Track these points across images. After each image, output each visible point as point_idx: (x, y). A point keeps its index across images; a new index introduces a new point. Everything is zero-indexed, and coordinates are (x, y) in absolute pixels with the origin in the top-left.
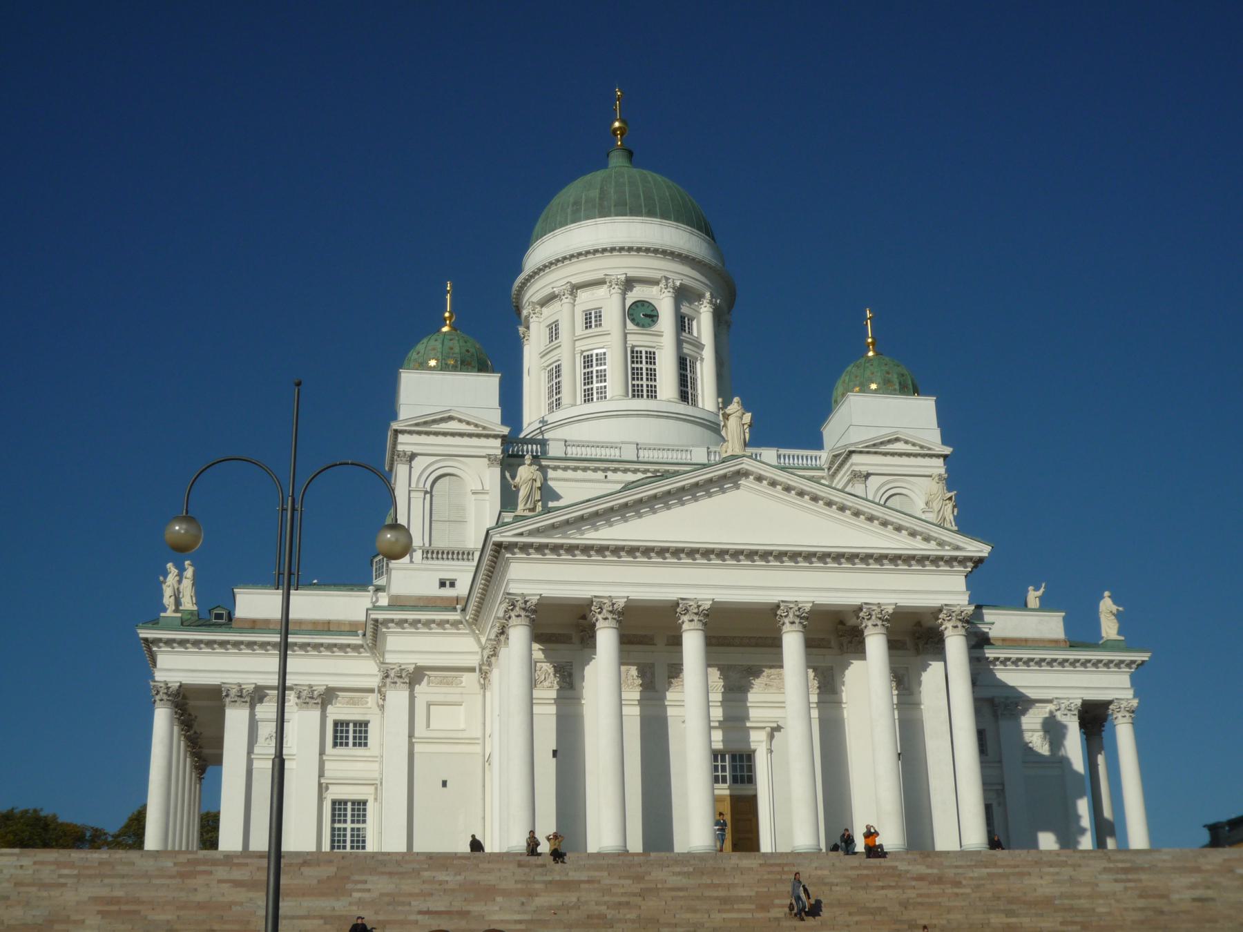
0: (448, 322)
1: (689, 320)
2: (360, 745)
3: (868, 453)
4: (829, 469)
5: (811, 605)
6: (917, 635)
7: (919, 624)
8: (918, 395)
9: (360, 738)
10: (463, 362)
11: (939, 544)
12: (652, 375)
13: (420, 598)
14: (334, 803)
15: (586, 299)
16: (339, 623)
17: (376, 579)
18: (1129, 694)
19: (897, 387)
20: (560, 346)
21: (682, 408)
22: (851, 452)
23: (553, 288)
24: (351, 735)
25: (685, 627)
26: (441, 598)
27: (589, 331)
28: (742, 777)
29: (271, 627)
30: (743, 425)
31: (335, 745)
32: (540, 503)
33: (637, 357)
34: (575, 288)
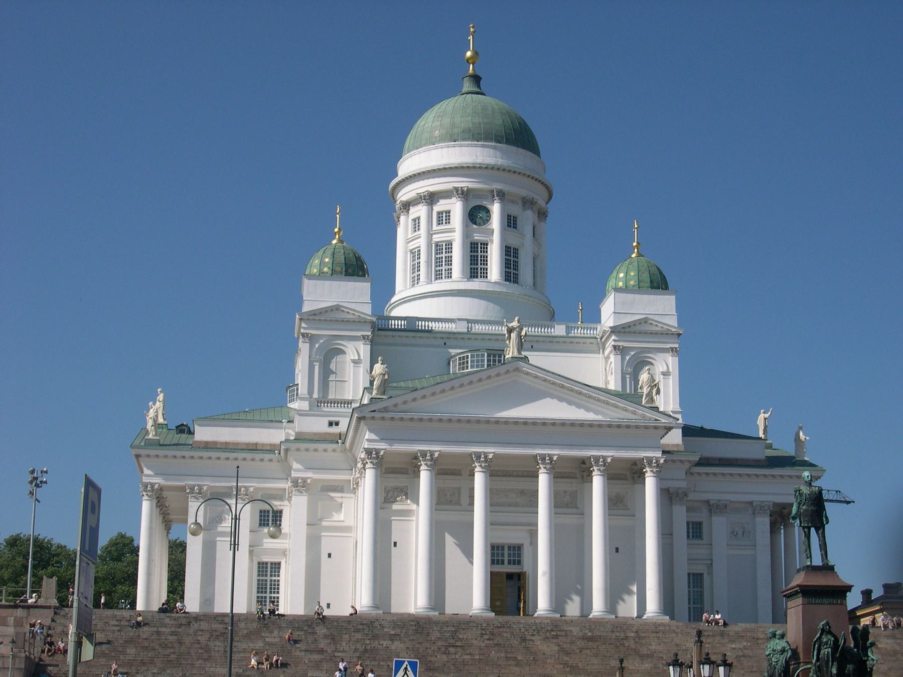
0: (337, 236)
1: (514, 217)
3: (625, 332)
4: (601, 338)
6: (633, 471)
8: (666, 288)
10: (346, 271)
12: (485, 261)
13: (315, 434)
16: (263, 445)
17: (289, 403)
19: (649, 284)
20: (420, 237)
23: (417, 194)
26: (330, 434)
27: (441, 227)
28: (514, 561)
29: (218, 446)
31: (260, 525)
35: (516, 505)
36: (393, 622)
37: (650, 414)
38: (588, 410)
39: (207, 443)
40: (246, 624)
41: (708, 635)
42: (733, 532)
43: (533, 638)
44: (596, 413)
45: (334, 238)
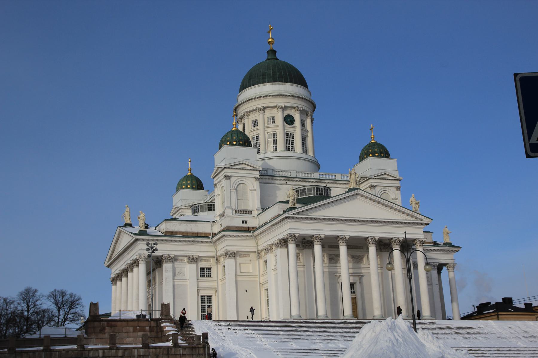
2: (208, 276)
3: (376, 178)
5: (378, 238)
9: (208, 274)
11: (416, 219)
12: (293, 142)
13: (237, 227)
15: (268, 113)
16: (201, 233)
21: (304, 156)
22: (371, 178)
24: (205, 272)
25: (340, 244)
32: (296, 203)
33: (288, 136)
34: (265, 108)
37: (419, 216)
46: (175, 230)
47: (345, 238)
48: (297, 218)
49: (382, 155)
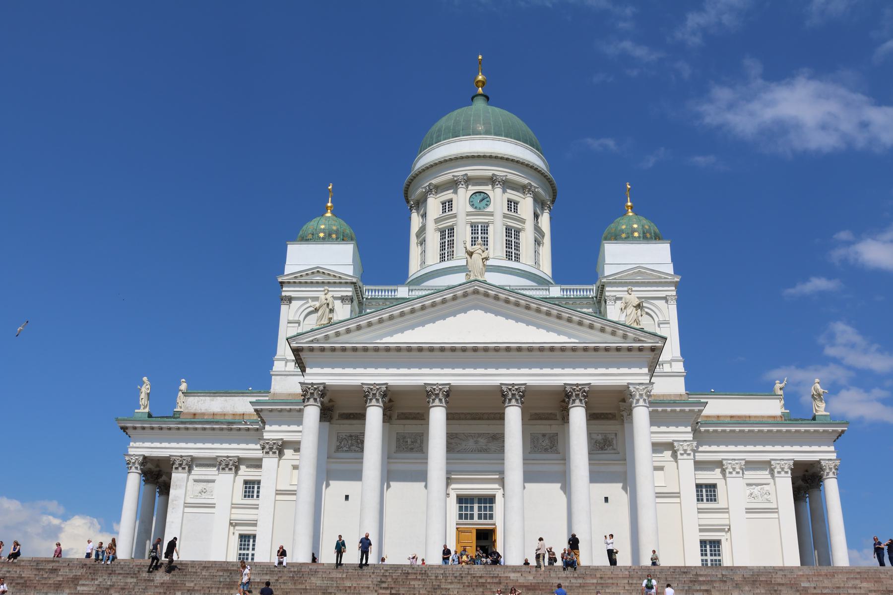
0: (329, 211)
1: (514, 203)
7: (624, 401)
13: (289, 395)
14: (239, 534)
16: (250, 415)
18: (833, 456)
19: (641, 235)
25: (431, 405)
30: (483, 259)
31: (245, 496)
33: (475, 230)
35: (485, 451)
36: (267, 568)
38: (559, 333)
39: (195, 414)
40: (111, 579)
41: (704, 581)
42: (751, 494)
43: (452, 586)
44: (570, 336)
45: (326, 212)
46: (201, 410)
47: (441, 389)
48: (323, 350)
49: (636, 234)
